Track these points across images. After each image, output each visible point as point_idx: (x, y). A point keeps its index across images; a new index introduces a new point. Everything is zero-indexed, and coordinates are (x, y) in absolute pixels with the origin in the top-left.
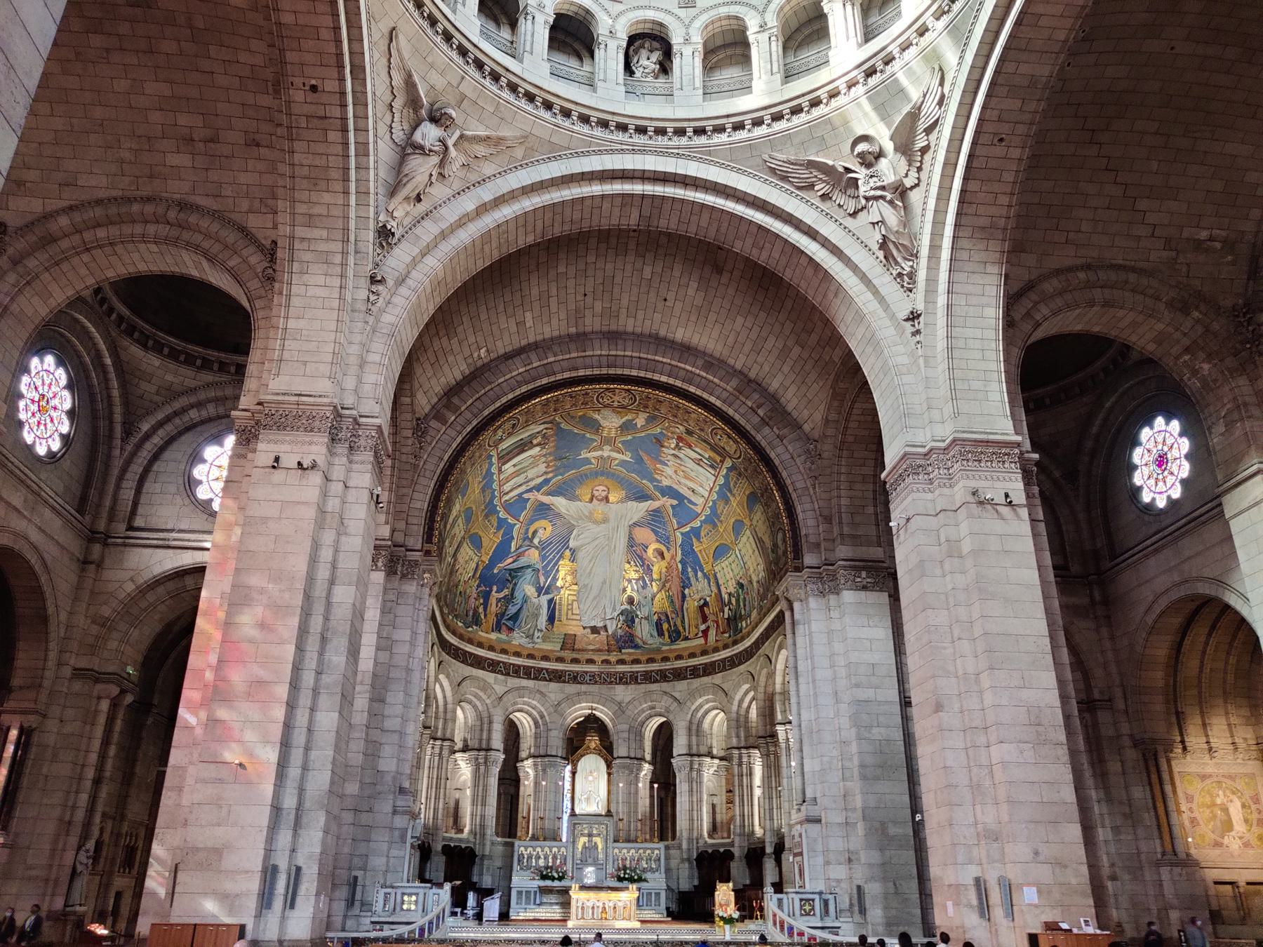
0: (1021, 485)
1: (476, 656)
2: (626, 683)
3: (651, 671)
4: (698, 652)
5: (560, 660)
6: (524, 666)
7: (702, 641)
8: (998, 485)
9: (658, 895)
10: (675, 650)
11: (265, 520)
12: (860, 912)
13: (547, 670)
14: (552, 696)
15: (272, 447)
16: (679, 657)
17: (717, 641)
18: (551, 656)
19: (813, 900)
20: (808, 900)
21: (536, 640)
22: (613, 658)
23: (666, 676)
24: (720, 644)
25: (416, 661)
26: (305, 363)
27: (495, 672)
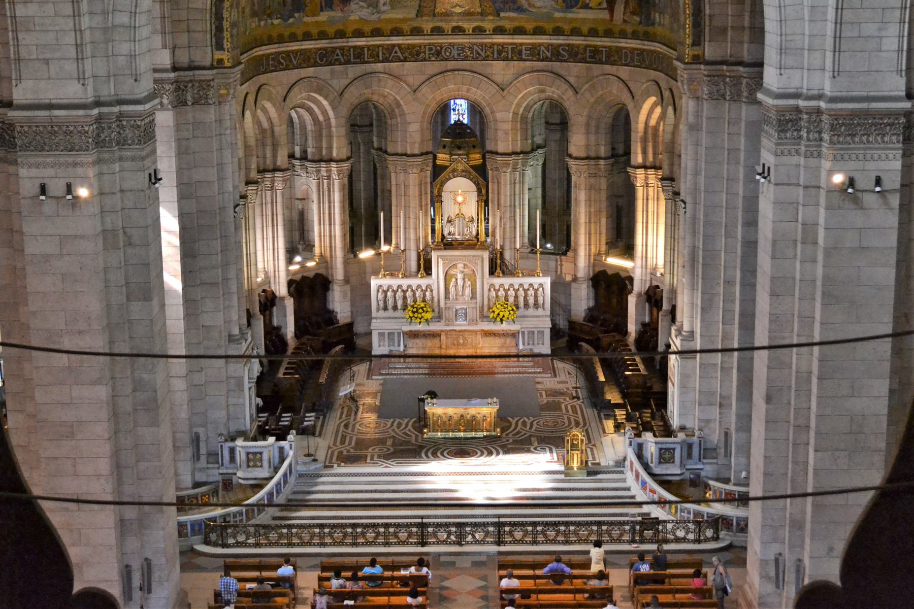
0: (897, 165)
1: (303, 52)
2: (506, 59)
3: (540, 45)
4: (601, 29)
5: (417, 31)
6: (369, 47)
7: (605, 15)
8: (870, 165)
9: (541, 333)
10: (571, 21)
11: (47, 258)
12: (726, 456)
13: (399, 46)
14: (410, 80)
15: (34, 172)
16: (575, 32)
17: (625, 21)
18: (406, 27)
19: (674, 449)
20: (668, 449)
21: (383, 8)
22: (488, 25)
23: (559, 54)
24: (629, 29)
25: (226, 195)
26: (47, 62)
27: (330, 64)
